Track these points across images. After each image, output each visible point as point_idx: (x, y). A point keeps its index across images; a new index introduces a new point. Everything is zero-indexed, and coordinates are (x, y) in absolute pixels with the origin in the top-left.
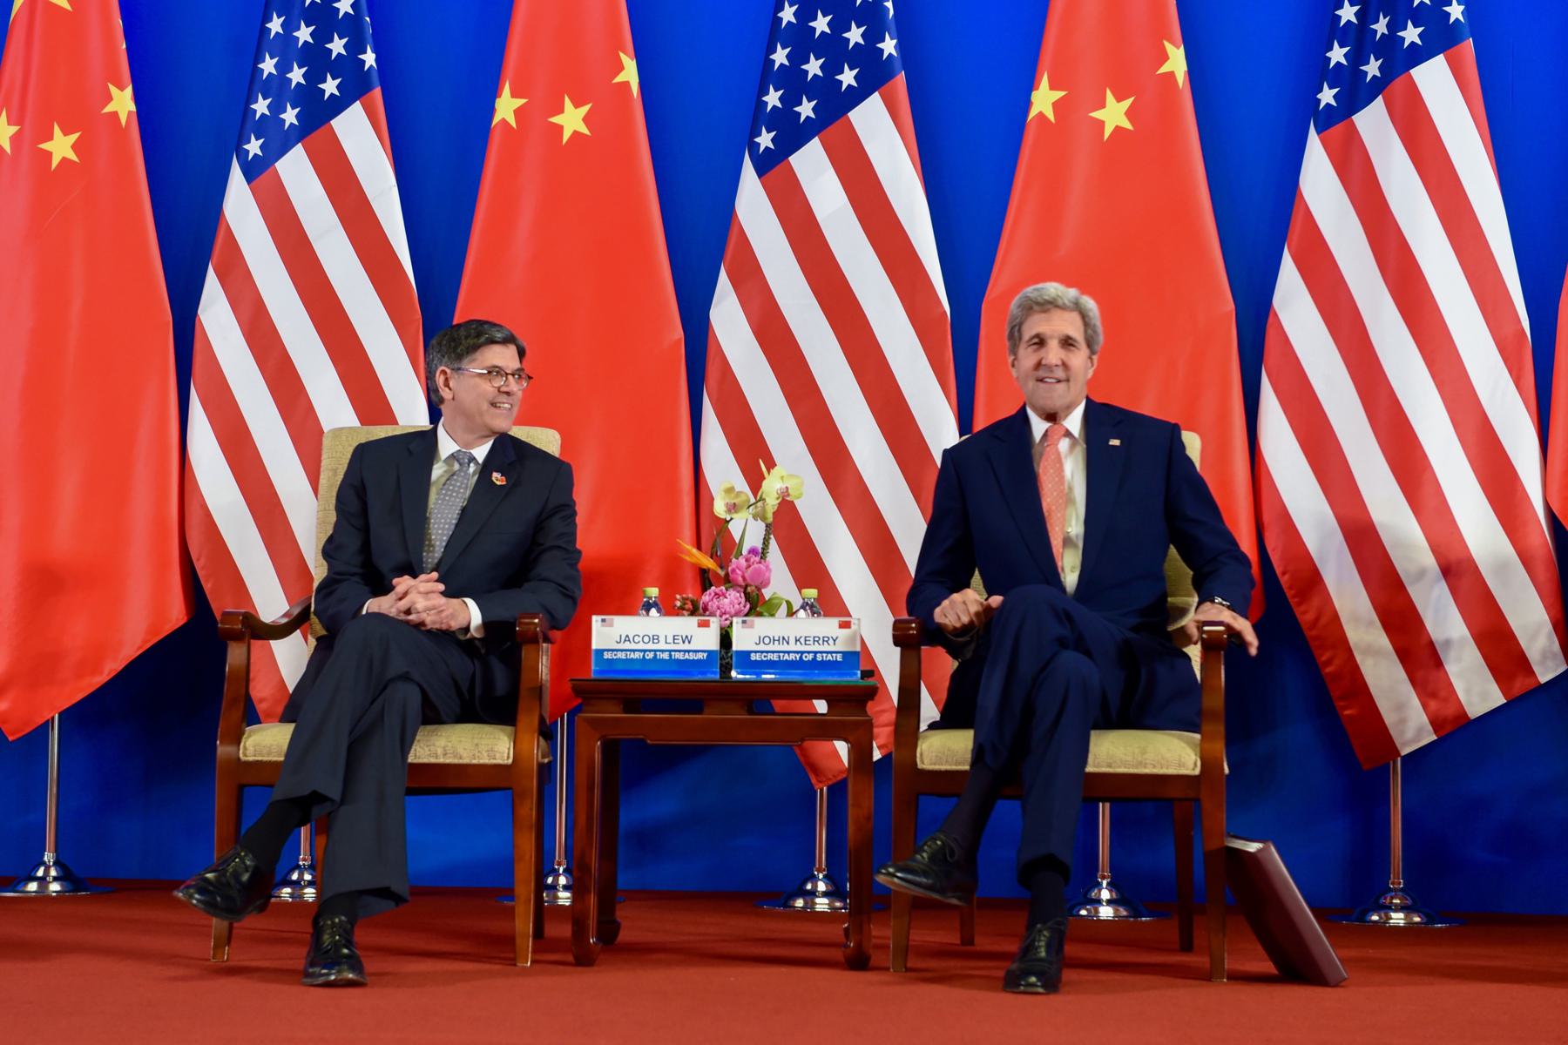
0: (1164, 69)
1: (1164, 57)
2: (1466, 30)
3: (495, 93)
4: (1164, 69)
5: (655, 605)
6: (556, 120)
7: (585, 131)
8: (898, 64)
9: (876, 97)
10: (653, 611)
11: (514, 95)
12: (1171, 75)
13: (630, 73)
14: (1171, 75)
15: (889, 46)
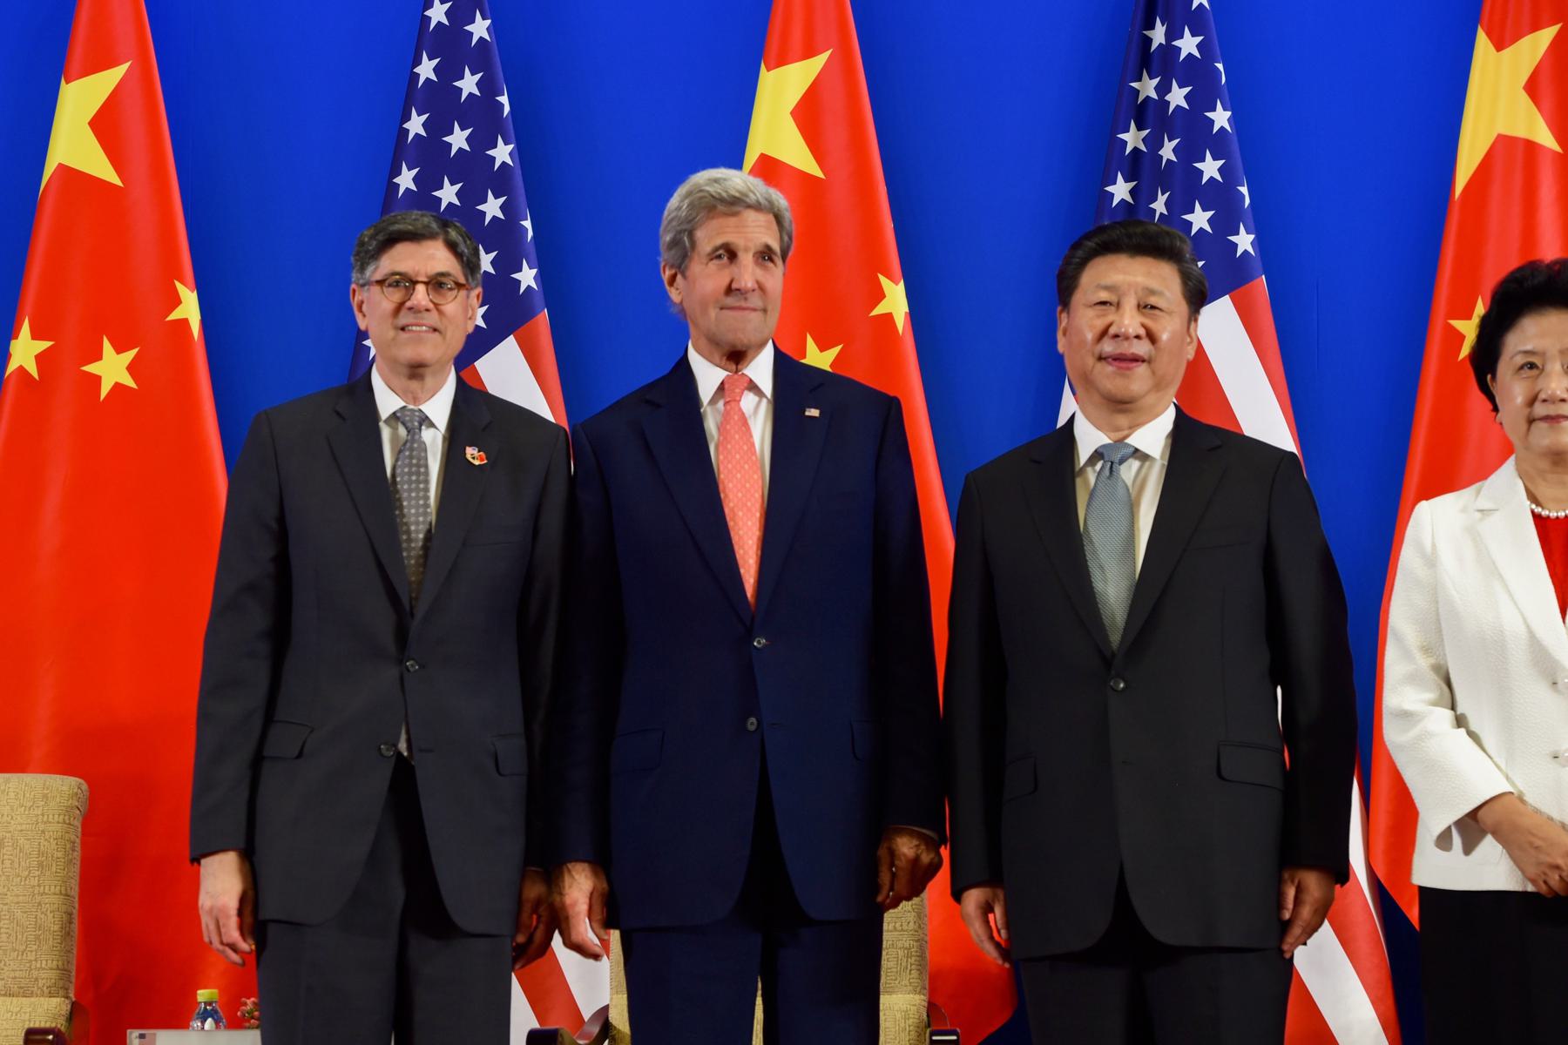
0: (879, 310)
1: (880, 295)
2: (1258, 265)
3: (13, 333)
4: (879, 310)
5: (212, 1014)
6: (91, 368)
7: (131, 383)
8: (539, 300)
9: (511, 341)
10: (209, 1023)
11: (36, 336)
12: (888, 318)
13: (189, 308)
14: (888, 318)
15: (527, 277)
